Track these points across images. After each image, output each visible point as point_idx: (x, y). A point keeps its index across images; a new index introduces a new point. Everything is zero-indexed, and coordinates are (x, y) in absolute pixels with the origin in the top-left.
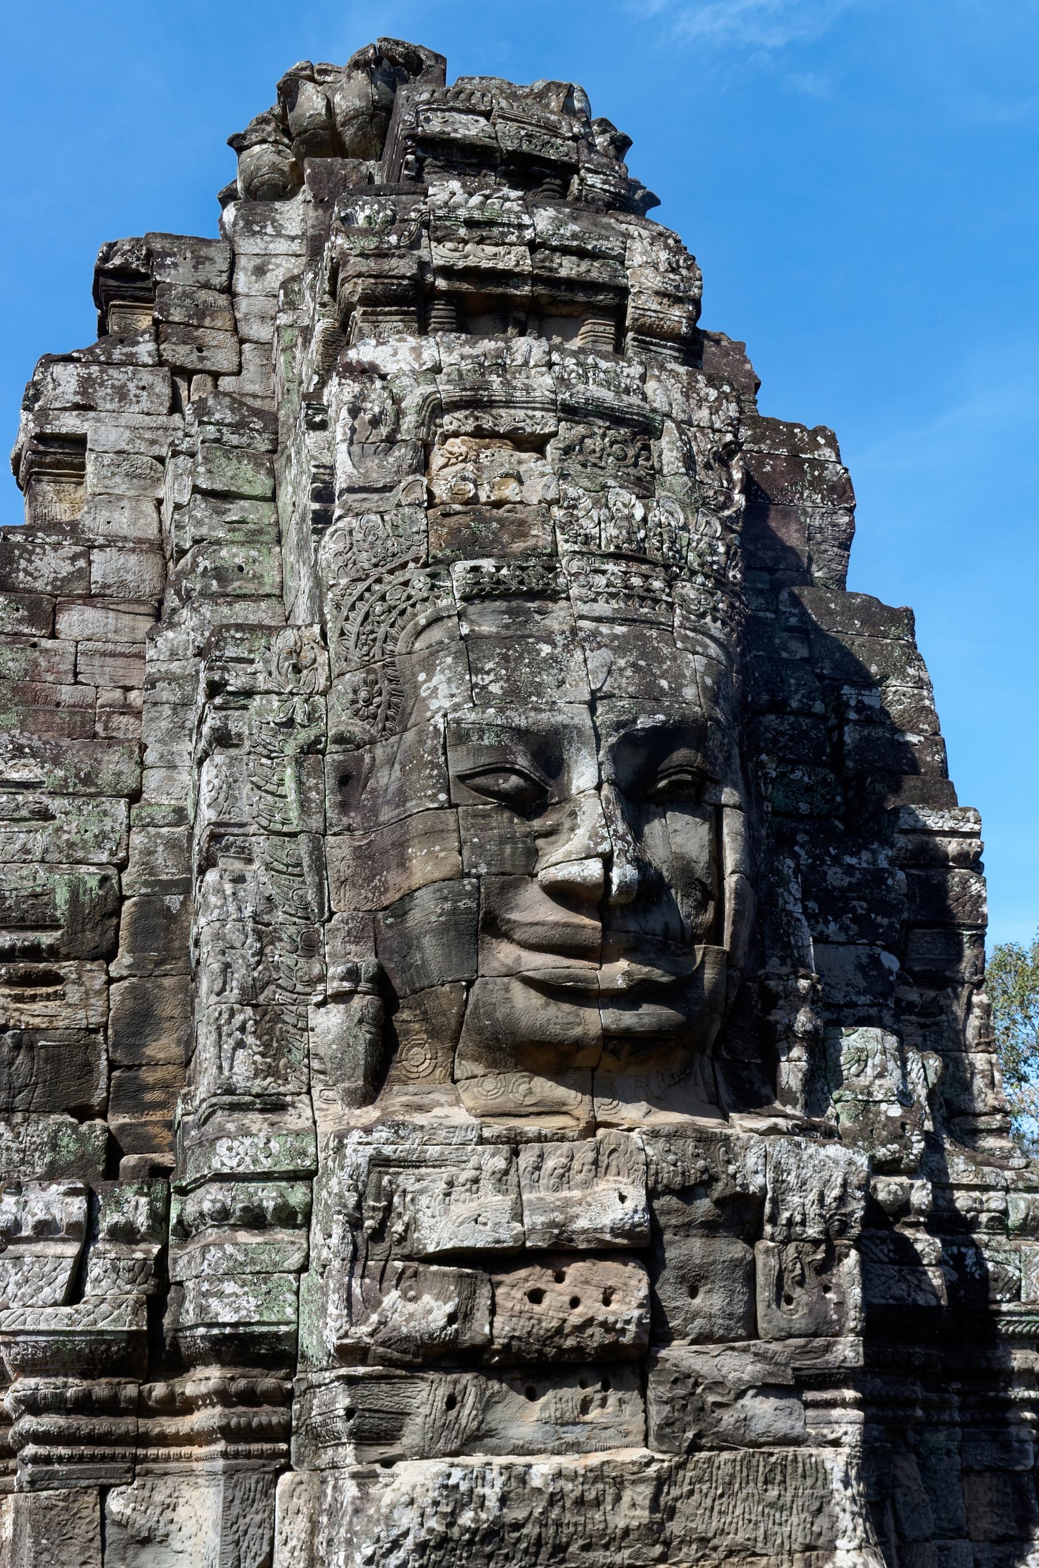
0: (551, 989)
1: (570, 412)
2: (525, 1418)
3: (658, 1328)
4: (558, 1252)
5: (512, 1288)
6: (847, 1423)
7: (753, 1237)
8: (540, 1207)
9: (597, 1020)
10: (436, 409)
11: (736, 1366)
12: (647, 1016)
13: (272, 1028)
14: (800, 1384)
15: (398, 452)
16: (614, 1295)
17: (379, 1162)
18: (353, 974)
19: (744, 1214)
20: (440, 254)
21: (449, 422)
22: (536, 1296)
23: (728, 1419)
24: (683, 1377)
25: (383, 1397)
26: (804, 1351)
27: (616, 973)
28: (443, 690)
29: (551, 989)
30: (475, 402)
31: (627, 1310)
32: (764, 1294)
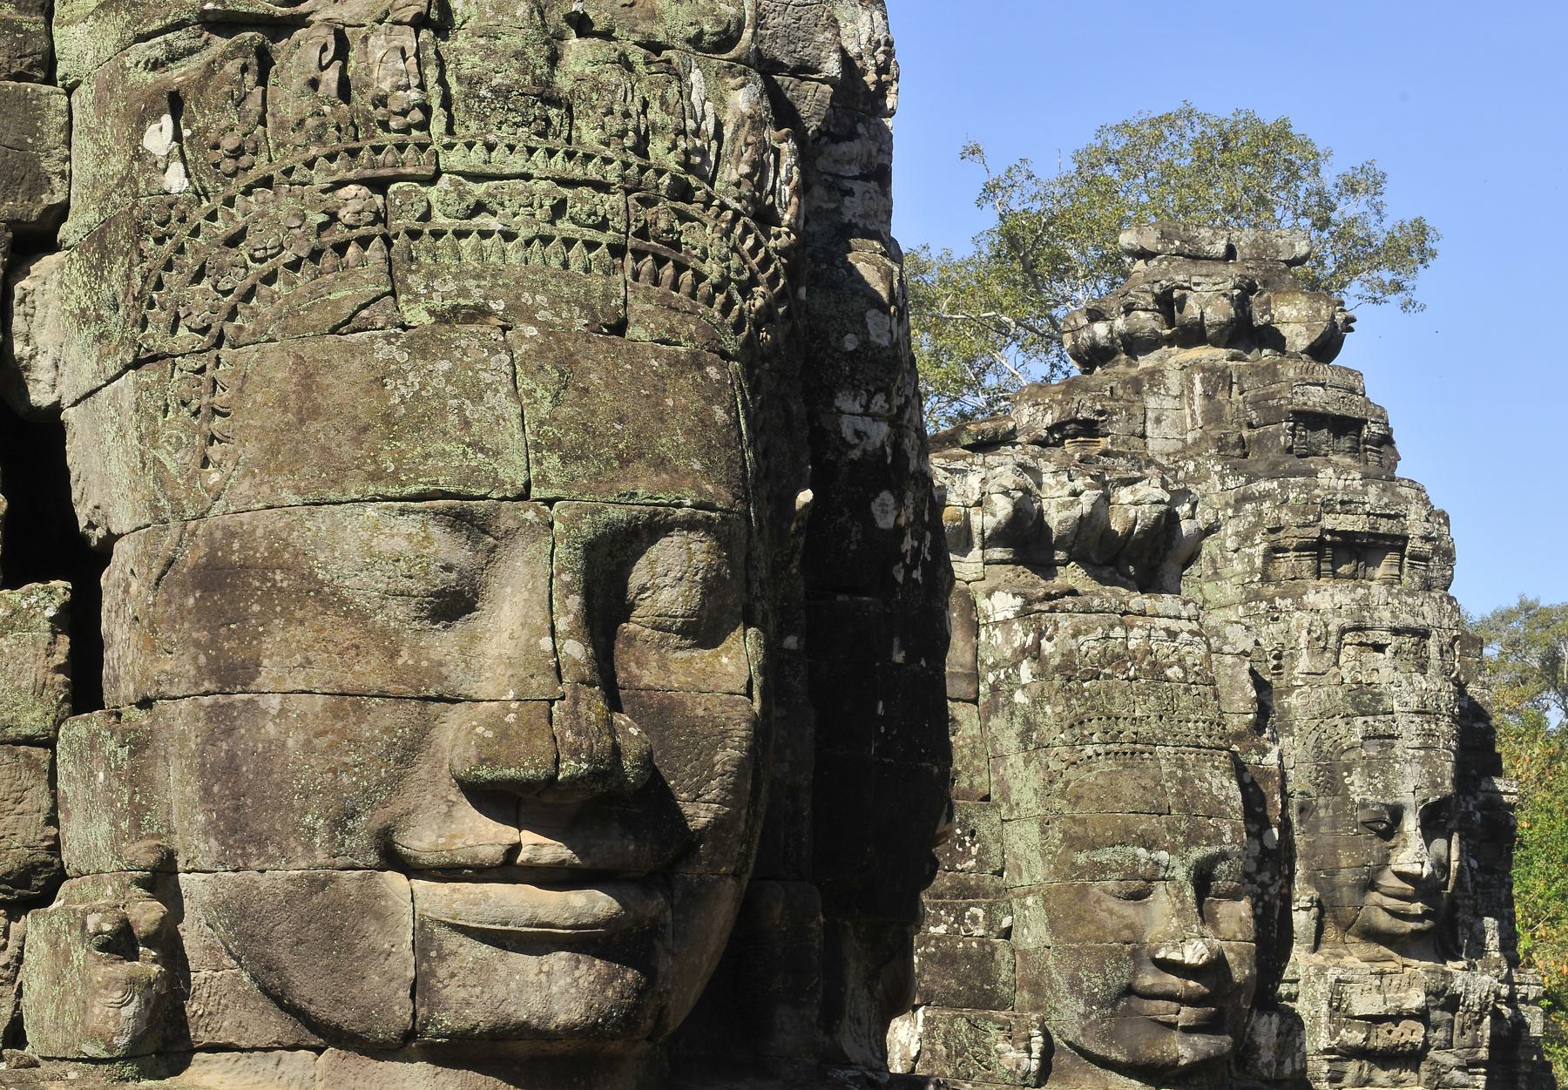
0: (1394, 914)
1: (1396, 632)
3: (1427, 1046)
4: (1397, 1018)
5: (1382, 1029)
7: (1454, 1010)
8: (1392, 1000)
9: (1411, 926)
11: (1448, 1058)
12: (1428, 923)
14: (1469, 1066)
15: (1328, 655)
16: (1413, 1033)
17: (1338, 981)
18: (1311, 901)
20: (1329, 522)
21: (1348, 638)
22: (1390, 1032)
23: (1447, 1077)
24: (1434, 1062)
25: (1339, 1066)
26: (1469, 1054)
27: (1417, 908)
28: (1357, 783)
29: (1394, 914)
30: (1359, 629)
31: (1418, 1038)
32: (1457, 1032)
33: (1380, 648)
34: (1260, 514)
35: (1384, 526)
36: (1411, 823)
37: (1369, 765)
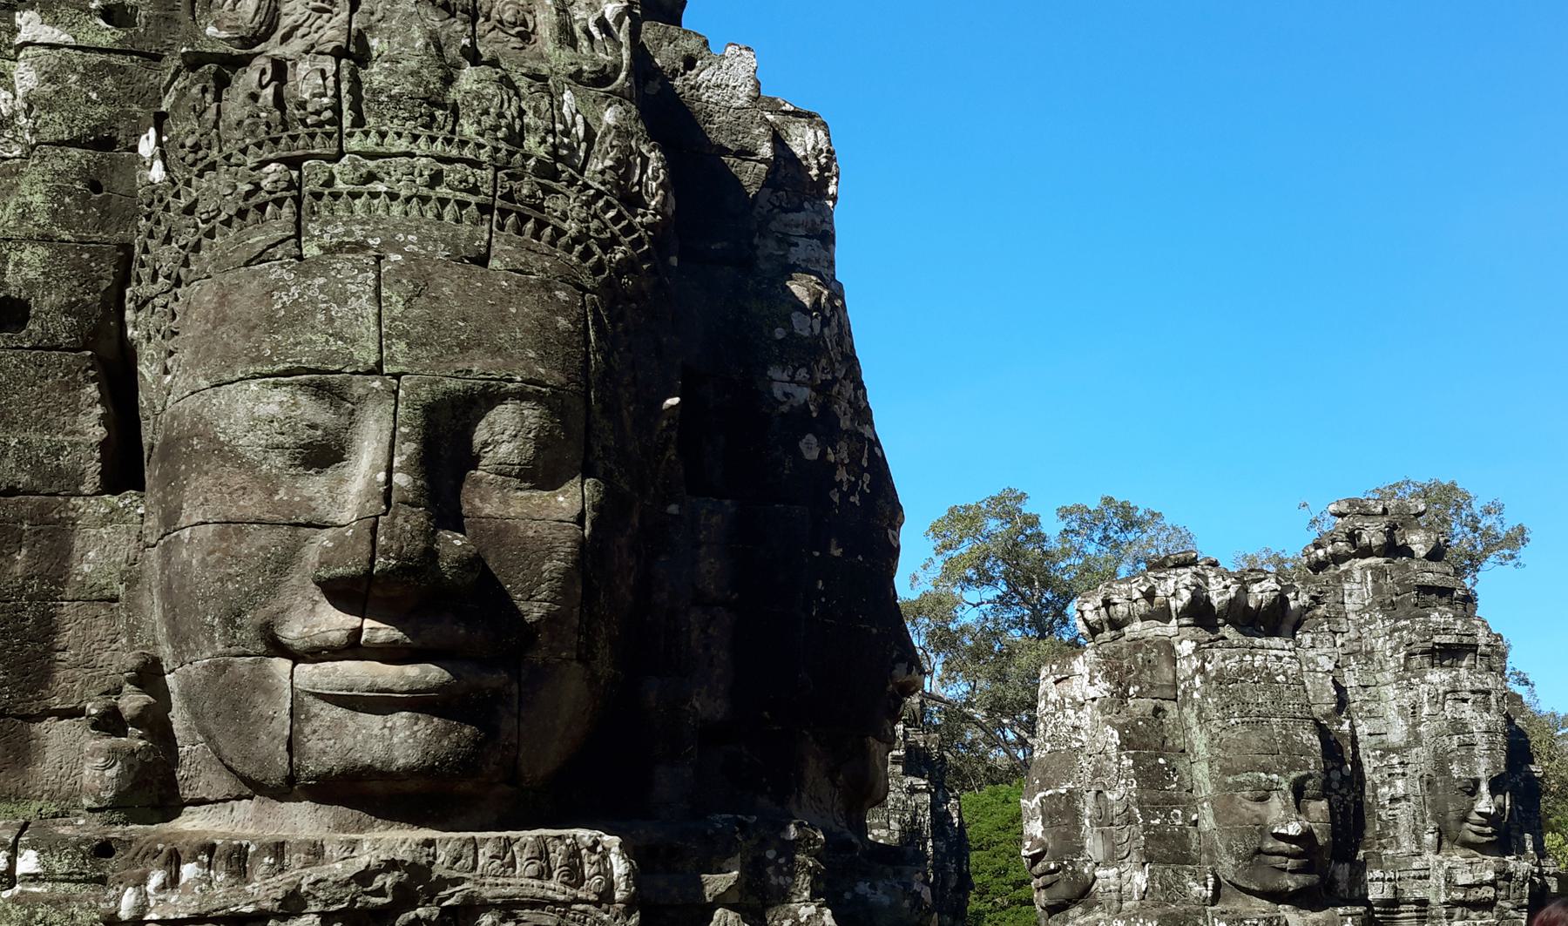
0: (1476, 833)
1: (1473, 692)
2: (1473, 915)
3: (1496, 898)
4: (1480, 885)
5: (1473, 892)
6: (1525, 915)
10: (1446, 693)
11: (1508, 905)
13: (1418, 840)
16: (1489, 893)
19: (1509, 877)
20: (1437, 639)
27: (1489, 830)
29: (1476, 833)
30: (1454, 691)
31: (1491, 895)
33: (1465, 701)
34: (1401, 637)
35: (1466, 640)
36: (1484, 788)
37: (1461, 760)
